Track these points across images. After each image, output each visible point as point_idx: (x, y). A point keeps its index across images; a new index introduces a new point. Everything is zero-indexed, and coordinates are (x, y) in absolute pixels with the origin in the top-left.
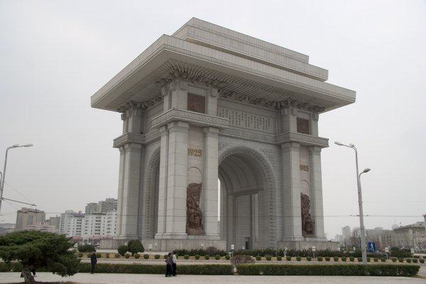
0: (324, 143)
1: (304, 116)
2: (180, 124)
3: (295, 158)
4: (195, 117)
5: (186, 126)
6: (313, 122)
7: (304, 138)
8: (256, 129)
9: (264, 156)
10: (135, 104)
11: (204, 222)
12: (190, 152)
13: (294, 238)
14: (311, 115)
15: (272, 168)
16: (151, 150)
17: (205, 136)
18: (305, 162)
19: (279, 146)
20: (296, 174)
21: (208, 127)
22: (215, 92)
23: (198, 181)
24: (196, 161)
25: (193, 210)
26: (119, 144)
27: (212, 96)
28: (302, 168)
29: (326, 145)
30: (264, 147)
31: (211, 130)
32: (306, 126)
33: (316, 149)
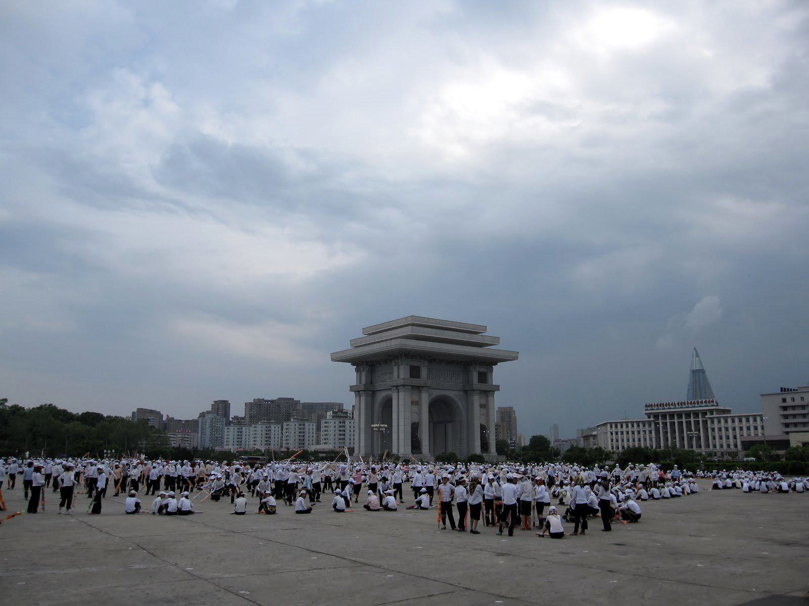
0: (497, 388)
1: (483, 370)
2: (406, 387)
3: (477, 400)
4: (415, 381)
5: (410, 388)
6: (489, 374)
7: (483, 387)
9: (457, 400)
10: (367, 362)
11: (421, 446)
12: (412, 403)
15: (461, 407)
16: (380, 396)
17: (420, 391)
18: (483, 402)
19: (466, 392)
20: (477, 410)
22: (426, 363)
23: (416, 420)
24: (415, 408)
25: (415, 439)
26: (352, 388)
28: (482, 406)
30: (456, 393)
32: (484, 378)
33: (490, 393)
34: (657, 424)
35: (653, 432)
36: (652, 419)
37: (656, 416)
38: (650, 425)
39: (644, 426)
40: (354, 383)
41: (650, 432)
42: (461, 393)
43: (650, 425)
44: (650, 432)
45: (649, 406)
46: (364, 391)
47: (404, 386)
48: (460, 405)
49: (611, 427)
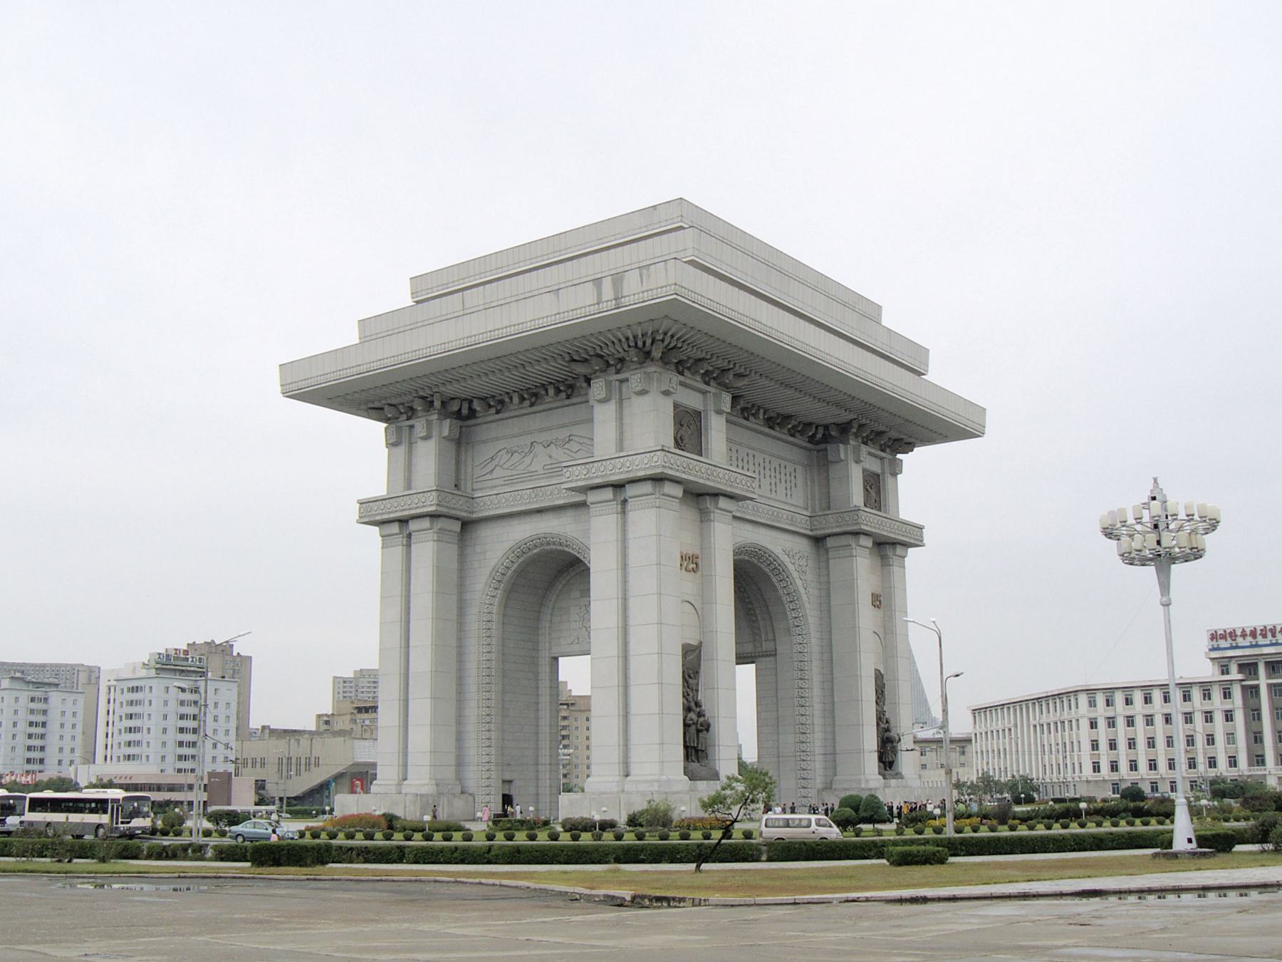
2: (669, 488)
6: (889, 479)
8: (773, 496)
9: (791, 567)
13: (867, 781)
14: (886, 462)
17: (704, 516)
19: (818, 541)
21: (716, 495)
27: (719, 412)
29: (918, 543)
31: (723, 503)
33: (899, 550)
34: (1251, 692)
35: (1239, 716)
36: (1235, 674)
37: (1248, 668)
38: (1227, 695)
39: (1207, 695)
40: (378, 487)
41: (1229, 716)
42: (803, 546)
43: (1227, 695)
44: (1229, 716)
45: (1223, 637)
46: (433, 516)
47: (658, 479)
48: (802, 591)
49: (1092, 704)
